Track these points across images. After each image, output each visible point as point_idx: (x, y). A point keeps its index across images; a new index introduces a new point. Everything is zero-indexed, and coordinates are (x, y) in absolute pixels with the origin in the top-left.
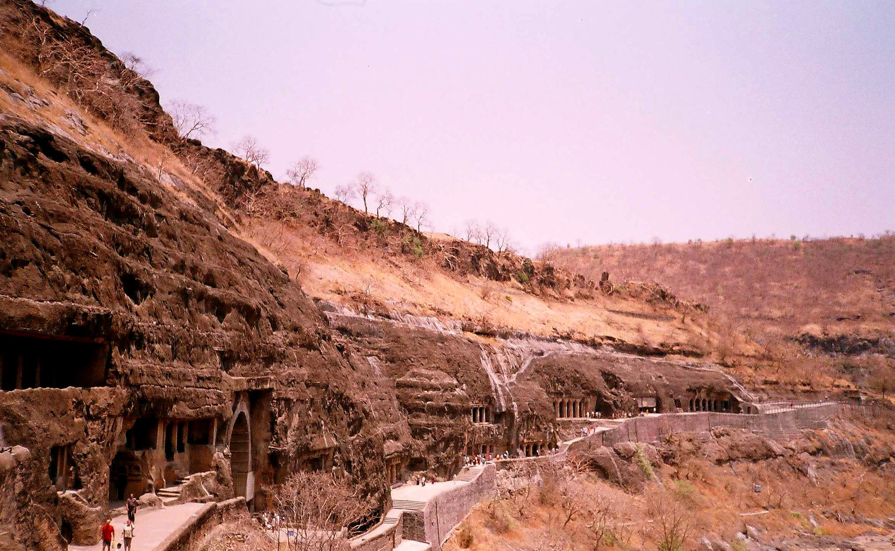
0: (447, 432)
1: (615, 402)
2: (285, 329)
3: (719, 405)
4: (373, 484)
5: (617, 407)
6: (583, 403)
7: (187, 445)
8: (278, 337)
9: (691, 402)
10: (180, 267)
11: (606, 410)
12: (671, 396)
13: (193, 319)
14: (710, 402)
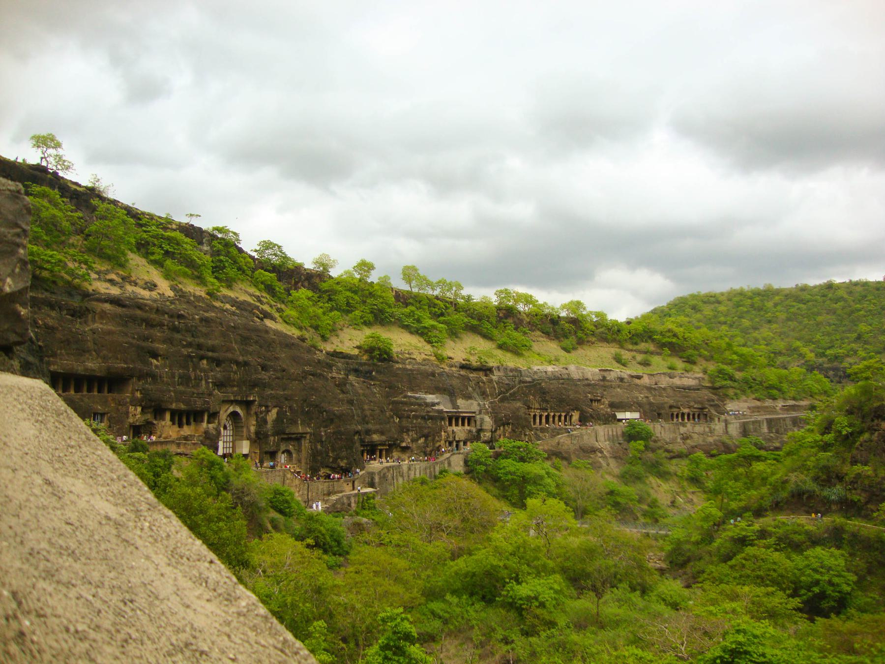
0: (426, 431)
2: (275, 370)
3: (702, 416)
4: (344, 454)
6: (568, 417)
7: (193, 423)
8: (264, 376)
10: (190, 345)
11: (583, 420)
13: (195, 368)
14: (694, 415)
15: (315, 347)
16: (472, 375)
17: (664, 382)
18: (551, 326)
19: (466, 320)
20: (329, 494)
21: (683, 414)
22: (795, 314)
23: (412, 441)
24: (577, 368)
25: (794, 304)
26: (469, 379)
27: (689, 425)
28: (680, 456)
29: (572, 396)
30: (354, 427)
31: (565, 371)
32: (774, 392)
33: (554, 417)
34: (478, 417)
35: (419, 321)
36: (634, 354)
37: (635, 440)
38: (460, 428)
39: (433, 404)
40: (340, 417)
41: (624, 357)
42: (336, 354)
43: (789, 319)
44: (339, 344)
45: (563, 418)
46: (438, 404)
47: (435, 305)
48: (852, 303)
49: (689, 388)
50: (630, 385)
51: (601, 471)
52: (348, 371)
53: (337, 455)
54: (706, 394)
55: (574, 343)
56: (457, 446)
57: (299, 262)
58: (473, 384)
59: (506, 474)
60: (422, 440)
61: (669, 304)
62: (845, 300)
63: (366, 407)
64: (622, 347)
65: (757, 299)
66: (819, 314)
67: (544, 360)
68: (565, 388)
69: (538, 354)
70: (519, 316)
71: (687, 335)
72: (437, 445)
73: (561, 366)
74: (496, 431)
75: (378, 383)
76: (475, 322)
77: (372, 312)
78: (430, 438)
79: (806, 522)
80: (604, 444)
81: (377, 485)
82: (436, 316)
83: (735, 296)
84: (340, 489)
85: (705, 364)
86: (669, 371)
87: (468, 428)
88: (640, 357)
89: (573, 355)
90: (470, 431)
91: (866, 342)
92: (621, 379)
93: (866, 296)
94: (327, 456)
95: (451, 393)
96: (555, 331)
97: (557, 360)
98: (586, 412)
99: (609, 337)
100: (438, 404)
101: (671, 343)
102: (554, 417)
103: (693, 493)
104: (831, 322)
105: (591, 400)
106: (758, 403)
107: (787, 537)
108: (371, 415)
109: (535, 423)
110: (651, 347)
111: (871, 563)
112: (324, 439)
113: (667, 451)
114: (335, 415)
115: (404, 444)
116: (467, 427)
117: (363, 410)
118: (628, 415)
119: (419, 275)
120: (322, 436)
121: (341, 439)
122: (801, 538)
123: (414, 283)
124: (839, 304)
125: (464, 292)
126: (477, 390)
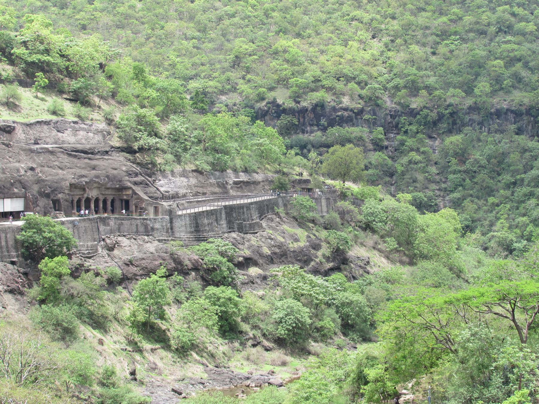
3: (117, 204)
9: (79, 201)
12: (48, 196)
14: (105, 202)
17: (50, 139)
21: (88, 200)
22: (127, 17)
37: (52, 257)
54: (120, 164)
66: (166, 18)
86: (54, 118)
91: (248, 70)
103: (153, 350)
104: (189, 33)
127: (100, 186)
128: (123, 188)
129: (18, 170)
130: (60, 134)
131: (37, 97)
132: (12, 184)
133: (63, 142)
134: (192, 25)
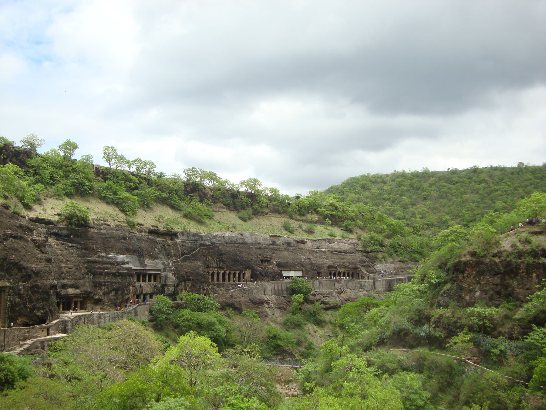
0: (116, 286)
1: (260, 273)
3: (355, 275)
4: (40, 305)
5: (262, 275)
11: (255, 277)
12: (315, 270)
15: (17, 214)
16: (159, 239)
17: (325, 246)
18: (232, 199)
19: (157, 193)
20: (25, 340)
22: (446, 193)
23: (105, 294)
24: (251, 234)
25: (446, 184)
26: (156, 242)
27: (343, 282)
28: (335, 308)
29: (245, 256)
30: (50, 281)
31: (241, 237)
32: (417, 255)
33: (229, 274)
34: (163, 274)
35: (115, 193)
36: (301, 223)
37: (297, 294)
38: (147, 283)
39: (123, 263)
40: (37, 274)
41: (292, 226)
42: (38, 221)
43: (441, 197)
44: (42, 212)
45: (237, 275)
46: (127, 263)
47: (130, 180)
48: (491, 185)
49: (345, 252)
50: (294, 249)
51: (267, 320)
52: (50, 234)
53: (34, 306)
54: (359, 257)
55: (250, 213)
56: (144, 299)
57: (11, 140)
58: (159, 246)
59: (184, 321)
60: (113, 293)
61: (343, 183)
62: (486, 182)
63: (63, 265)
64: (291, 217)
65: (415, 180)
66: (465, 193)
67: (224, 227)
68: (239, 250)
69: (219, 222)
70: (204, 191)
71: (346, 208)
72: (126, 297)
73: (238, 232)
74: (178, 285)
75: (74, 245)
76: (164, 195)
77: (74, 185)
78: (120, 292)
79: (399, 354)
80: (271, 297)
81: (69, 332)
82: (130, 189)
83: (398, 177)
84: (34, 335)
85: (359, 232)
86: (329, 237)
87: (154, 283)
88: (305, 226)
89: (249, 224)
90: (155, 286)
92: (289, 244)
93: (502, 179)
94: (25, 307)
95: (139, 254)
96: (234, 203)
97: (235, 227)
98: (256, 271)
99: (280, 209)
100: (127, 263)
101: (332, 215)
102: (229, 274)
104: (475, 199)
105: (262, 261)
106: (402, 265)
107: (384, 365)
108: (68, 272)
109: (213, 280)
110: (315, 217)
111: (442, 383)
112: (22, 292)
113: (323, 303)
114: (33, 271)
115: (97, 297)
116: (153, 283)
117: (60, 268)
118: (293, 273)
119: (117, 155)
120: (20, 290)
121: (38, 293)
122: (394, 366)
123: (113, 161)
124: (481, 185)
125: (157, 170)
126: (163, 251)
127: (345, 267)
128: (356, 268)
129: (301, 259)
130: (330, 245)
131: (326, 229)
132: (296, 265)
133: (332, 248)
134: (476, 196)
